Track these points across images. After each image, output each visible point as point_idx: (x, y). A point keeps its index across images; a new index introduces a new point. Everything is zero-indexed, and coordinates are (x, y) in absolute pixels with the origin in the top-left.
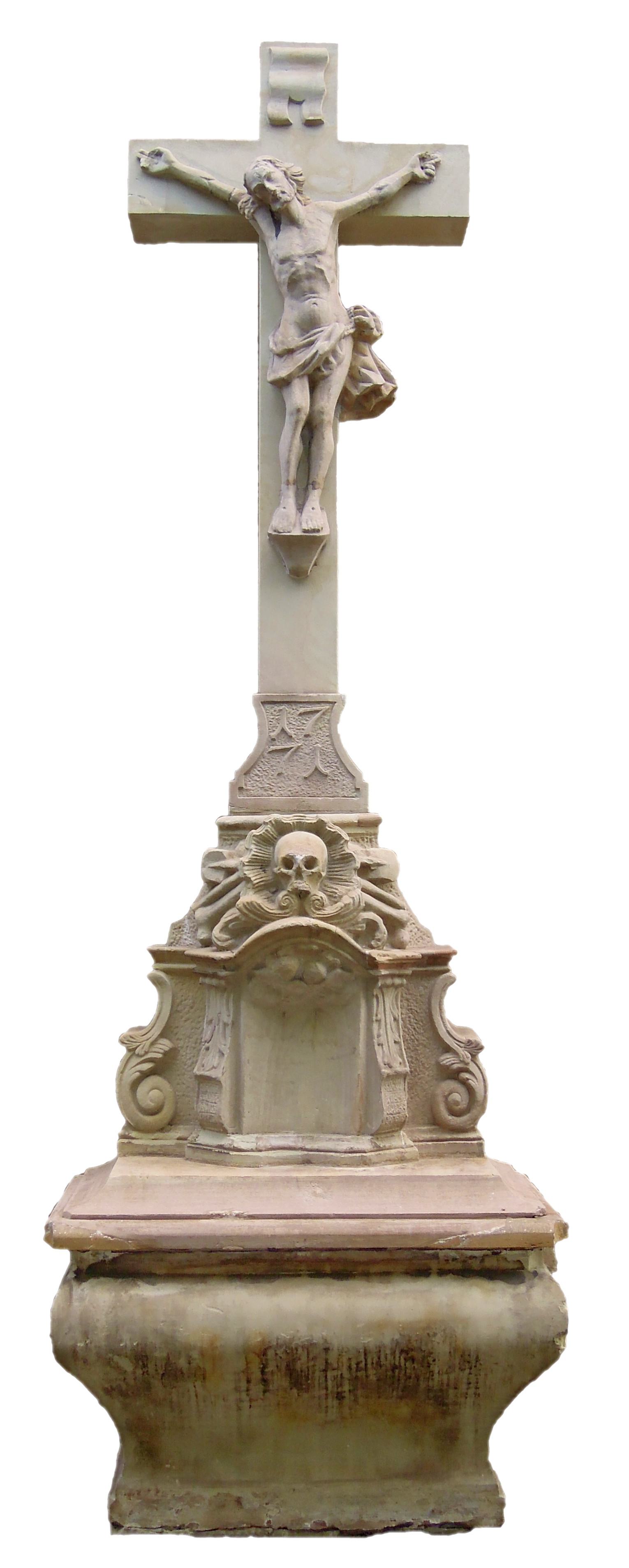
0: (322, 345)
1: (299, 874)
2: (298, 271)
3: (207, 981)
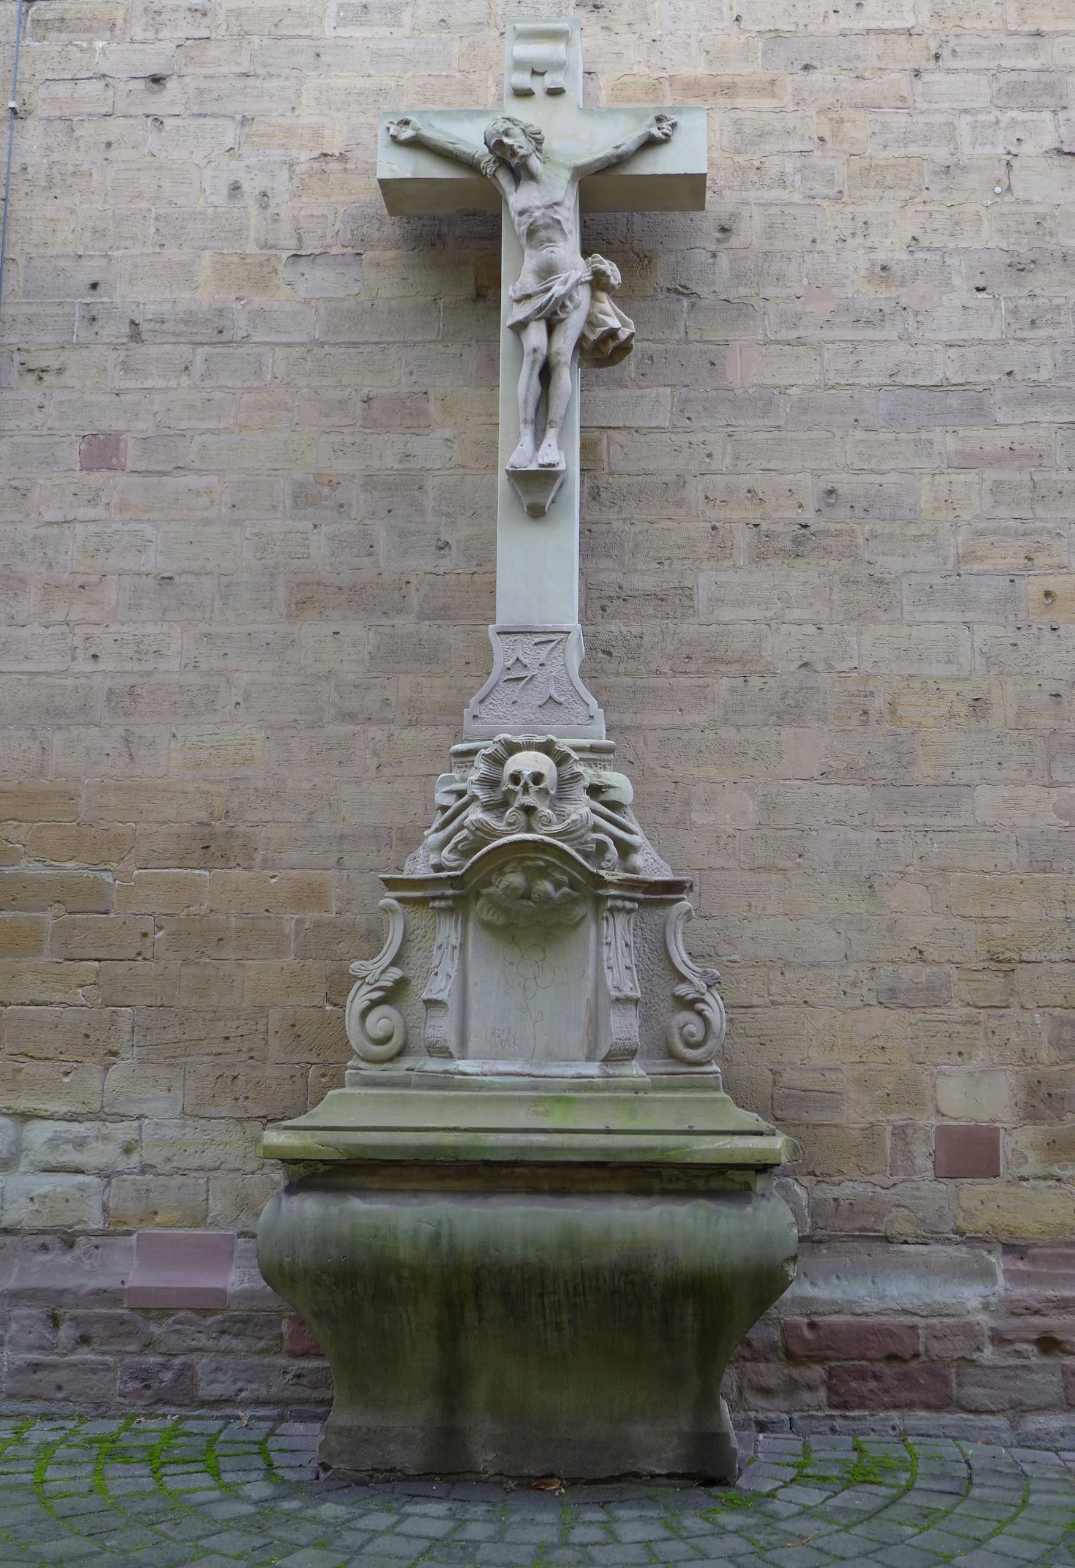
0: (558, 289)
1: (526, 790)
2: (535, 221)
3: (436, 904)
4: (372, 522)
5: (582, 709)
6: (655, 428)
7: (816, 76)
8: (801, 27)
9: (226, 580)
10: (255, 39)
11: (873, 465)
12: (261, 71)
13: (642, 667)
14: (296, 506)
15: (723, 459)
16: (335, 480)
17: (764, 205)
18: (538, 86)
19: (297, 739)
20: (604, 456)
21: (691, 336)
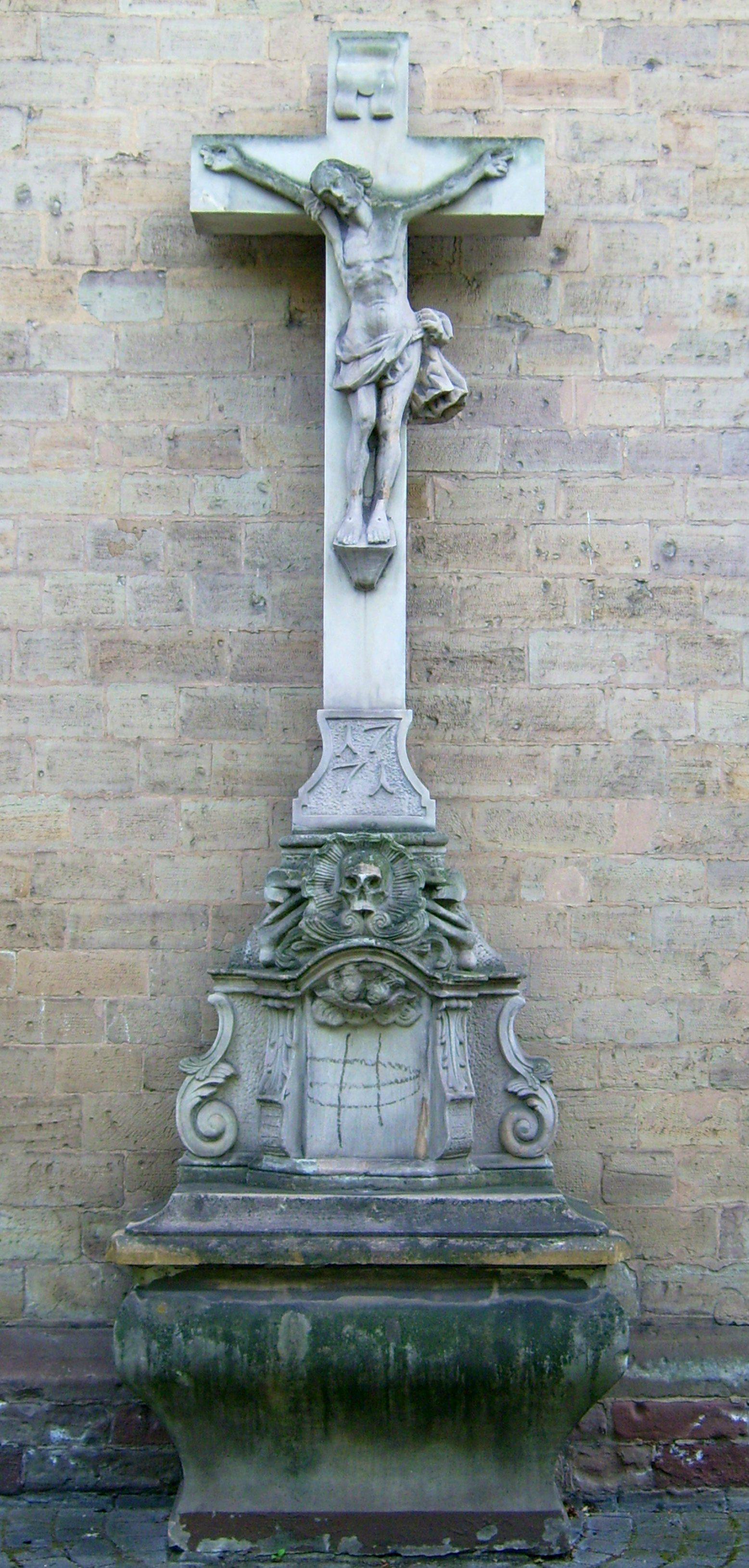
0: (388, 356)
1: (362, 893)
2: (364, 276)
3: (270, 1002)
4: (181, 574)
5: (415, 800)
6: (486, 473)
7: (660, 73)
8: (646, 15)
9: (26, 636)
10: (42, 17)
11: (714, 516)
12: (48, 54)
13: (469, 734)
14: (98, 555)
15: (556, 508)
16: (140, 527)
17: (603, 222)
18: (360, 108)
19: (105, 810)
20: (430, 504)
21: (522, 372)
